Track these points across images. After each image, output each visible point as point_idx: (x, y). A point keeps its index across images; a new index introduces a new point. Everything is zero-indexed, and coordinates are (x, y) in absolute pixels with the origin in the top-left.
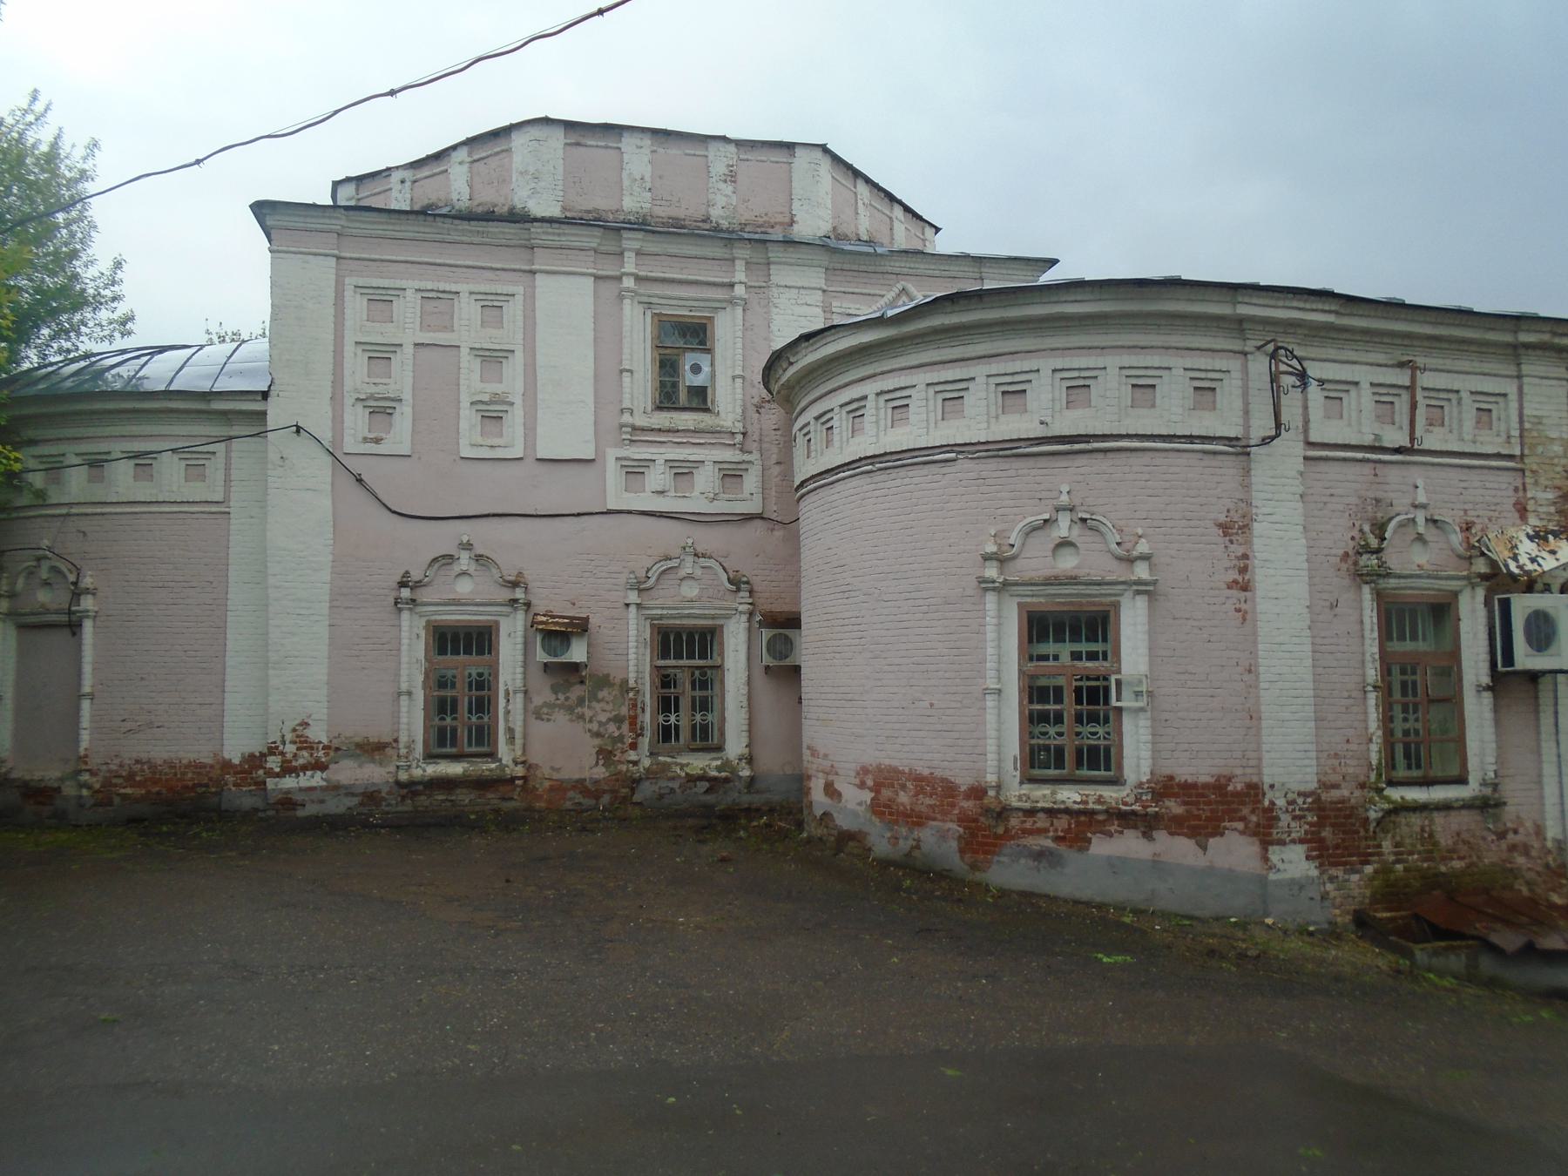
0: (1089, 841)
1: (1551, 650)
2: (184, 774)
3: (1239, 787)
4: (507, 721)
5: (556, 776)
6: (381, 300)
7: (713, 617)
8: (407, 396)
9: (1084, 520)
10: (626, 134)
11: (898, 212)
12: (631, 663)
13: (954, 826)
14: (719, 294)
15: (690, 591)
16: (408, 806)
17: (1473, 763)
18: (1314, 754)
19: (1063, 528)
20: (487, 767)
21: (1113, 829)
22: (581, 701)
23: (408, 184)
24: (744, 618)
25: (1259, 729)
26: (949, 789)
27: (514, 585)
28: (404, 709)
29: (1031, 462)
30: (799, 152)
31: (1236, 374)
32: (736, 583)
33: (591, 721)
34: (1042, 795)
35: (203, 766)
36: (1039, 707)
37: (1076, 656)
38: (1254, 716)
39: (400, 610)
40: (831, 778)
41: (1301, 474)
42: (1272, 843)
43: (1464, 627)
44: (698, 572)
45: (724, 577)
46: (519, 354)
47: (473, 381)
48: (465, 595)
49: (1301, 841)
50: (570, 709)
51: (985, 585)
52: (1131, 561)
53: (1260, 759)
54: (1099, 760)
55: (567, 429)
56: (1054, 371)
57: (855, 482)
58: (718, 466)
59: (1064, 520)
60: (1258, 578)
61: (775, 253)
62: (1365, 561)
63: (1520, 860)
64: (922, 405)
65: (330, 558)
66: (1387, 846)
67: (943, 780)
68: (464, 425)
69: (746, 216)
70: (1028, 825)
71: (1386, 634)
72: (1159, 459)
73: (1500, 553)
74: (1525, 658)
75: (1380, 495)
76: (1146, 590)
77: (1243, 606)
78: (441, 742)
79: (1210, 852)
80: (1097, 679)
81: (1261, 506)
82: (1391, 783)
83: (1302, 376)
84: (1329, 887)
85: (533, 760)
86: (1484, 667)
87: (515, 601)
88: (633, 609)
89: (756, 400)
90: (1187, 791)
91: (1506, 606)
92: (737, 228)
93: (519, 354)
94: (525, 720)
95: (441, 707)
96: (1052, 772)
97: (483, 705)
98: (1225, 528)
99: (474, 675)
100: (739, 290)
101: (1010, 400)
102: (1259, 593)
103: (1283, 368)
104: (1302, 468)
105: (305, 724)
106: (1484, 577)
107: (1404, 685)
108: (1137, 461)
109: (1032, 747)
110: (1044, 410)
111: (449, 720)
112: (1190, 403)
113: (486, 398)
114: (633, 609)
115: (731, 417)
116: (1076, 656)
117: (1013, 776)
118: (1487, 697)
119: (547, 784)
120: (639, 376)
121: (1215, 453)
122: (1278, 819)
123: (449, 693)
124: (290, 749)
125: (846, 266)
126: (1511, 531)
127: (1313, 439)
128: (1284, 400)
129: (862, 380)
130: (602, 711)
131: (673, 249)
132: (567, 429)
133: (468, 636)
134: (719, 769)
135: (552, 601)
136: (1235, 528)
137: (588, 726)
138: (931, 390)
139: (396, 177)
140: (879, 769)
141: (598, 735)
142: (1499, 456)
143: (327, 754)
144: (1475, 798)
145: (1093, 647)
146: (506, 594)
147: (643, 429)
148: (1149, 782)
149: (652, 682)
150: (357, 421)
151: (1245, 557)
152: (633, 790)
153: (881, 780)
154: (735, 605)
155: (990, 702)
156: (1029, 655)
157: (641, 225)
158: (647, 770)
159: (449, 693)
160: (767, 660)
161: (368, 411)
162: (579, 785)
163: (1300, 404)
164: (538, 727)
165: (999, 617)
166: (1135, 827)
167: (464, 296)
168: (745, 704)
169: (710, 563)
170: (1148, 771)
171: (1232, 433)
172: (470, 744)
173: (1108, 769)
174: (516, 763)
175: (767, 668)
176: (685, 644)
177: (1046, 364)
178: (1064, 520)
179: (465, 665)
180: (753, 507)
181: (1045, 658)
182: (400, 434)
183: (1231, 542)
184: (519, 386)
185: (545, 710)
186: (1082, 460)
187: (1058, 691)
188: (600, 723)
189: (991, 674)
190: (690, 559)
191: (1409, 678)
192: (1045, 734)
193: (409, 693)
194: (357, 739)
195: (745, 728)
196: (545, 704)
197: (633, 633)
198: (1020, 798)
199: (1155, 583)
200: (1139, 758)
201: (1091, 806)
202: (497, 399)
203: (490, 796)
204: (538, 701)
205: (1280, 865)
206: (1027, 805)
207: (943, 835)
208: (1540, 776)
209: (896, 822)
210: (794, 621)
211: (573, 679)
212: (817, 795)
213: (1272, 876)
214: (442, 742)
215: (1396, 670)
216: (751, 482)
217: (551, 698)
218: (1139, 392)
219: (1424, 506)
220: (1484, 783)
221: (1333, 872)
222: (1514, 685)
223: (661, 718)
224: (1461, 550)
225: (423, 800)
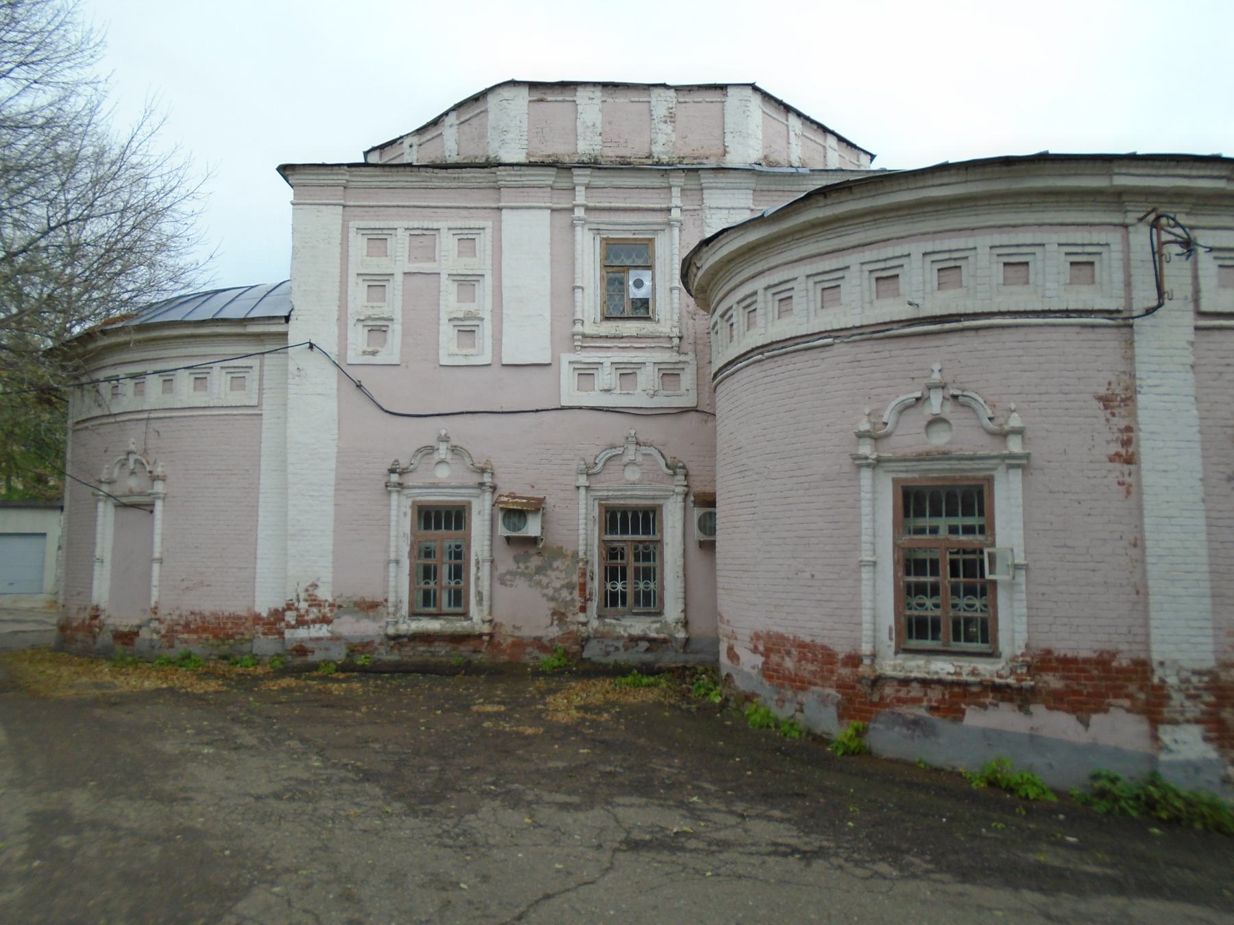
0: (963, 712)
2: (225, 624)
4: (477, 585)
5: (517, 633)
6: (378, 239)
8: (398, 316)
9: (955, 397)
10: (580, 90)
11: (832, 141)
12: (581, 538)
13: (833, 692)
14: (660, 218)
15: (632, 474)
16: (395, 657)
18: (1210, 632)
19: (935, 405)
20: (460, 625)
21: (988, 701)
22: (540, 570)
23: (415, 147)
24: (680, 498)
25: (1146, 605)
26: (829, 657)
27: (483, 471)
28: (392, 575)
29: (903, 343)
30: (730, 91)
31: (1117, 247)
32: (673, 467)
33: (547, 587)
34: (917, 666)
35: (239, 618)
38: (1141, 591)
39: (390, 492)
40: (732, 642)
41: (1192, 343)
42: (1162, 722)
44: (640, 459)
45: (663, 463)
46: (488, 280)
47: (451, 301)
48: (443, 481)
49: (1197, 721)
50: (529, 577)
51: (860, 463)
52: (1004, 435)
53: (1147, 635)
54: (979, 633)
55: (528, 337)
56: (925, 254)
57: (750, 370)
58: (658, 366)
59: (936, 398)
60: (1142, 450)
61: (706, 179)
64: (805, 296)
65: (335, 450)
67: (824, 647)
68: (442, 338)
69: (686, 151)
70: (902, 694)
72: (1033, 335)
76: (1021, 463)
77: (1127, 480)
78: (425, 602)
79: (1092, 729)
80: (974, 552)
83: (1188, 245)
85: (497, 620)
87: (482, 484)
88: (582, 491)
90: (1067, 664)
93: (488, 280)
94: (491, 585)
96: (928, 644)
97: (458, 572)
98: (1106, 401)
100: (676, 214)
101: (884, 285)
103: (1165, 237)
104: (1192, 338)
105: (315, 586)
108: (1006, 335)
109: (910, 619)
110: (921, 291)
111: (432, 584)
112: (1066, 277)
113: (461, 315)
115: (669, 323)
116: (953, 530)
117: (888, 645)
119: (510, 640)
121: (1093, 326)
122: (1169, 697)
124: (303, 605)
125: (773, 187)
127: (1206, 306)
128: (1168, 270)
129: (753, 277)
130: (556, 578)
131: (618, 181)
132: (528, 337)
133: (448, 514)
134: (658, 631)
135: (515, 485)
136: (1119, 400)
137: (545, 591)
138: (811, 281)
139: (407, 142)
140: (769, 635)
141: (552, 599)
143: (331, 611)
146: (476, 479)
147: (592, 337)
148: (1023, 655)
149: (600, 554)
150: (358, 338)
151: (1129, 429)
152: (583, 647)
153: (770, 645)
154: (672, 487)
155: (866, 574)
157: (593, 165)
158: (596, 631)
159: (431, 561)
161: (367, 329)
162: (538, 642)
163: (1189, 273)
164: (501, 591)
165: (874, 492)
166: (1011, 700)
167: (444, 232)
169: (652, 451)
170: (1022, 644)
171: (1112, 306)
172: (450, 605)
174: (484, 622)
176: (630, 522)
177: (916, 248)
178: (936, 398)
179: (443, 538)
180: (689, 401)
181: (921, 531)
182: (392, 350)
183: (1113, 415)
184: (488, 304)
185: (508, 577)
186: (953, 339)
187: (935, 564)
188: (556, 590)
189: (866, 547)
190: (632, 447)
192: (921, 605)
193: (397, 562)
194: (355, 599)
195: (681, 595)
196: (510, 573)
197: (582, 511)
198: (894, 668)
199: (1027, 456)
200: (1013, 631)
201: (965, 677)
202: (469, 316)
203: (462, 648)
204: (502, 569)
205: (1172, 746)
206: (901, 675)
207: (823, 700)
209: (782, 686)
211: (532, 551)
213: (1163, 757)
214: (426, 603)
216: (687, 379)
218: (1011, 270)
223: (609, 586)
225: (407, 651)
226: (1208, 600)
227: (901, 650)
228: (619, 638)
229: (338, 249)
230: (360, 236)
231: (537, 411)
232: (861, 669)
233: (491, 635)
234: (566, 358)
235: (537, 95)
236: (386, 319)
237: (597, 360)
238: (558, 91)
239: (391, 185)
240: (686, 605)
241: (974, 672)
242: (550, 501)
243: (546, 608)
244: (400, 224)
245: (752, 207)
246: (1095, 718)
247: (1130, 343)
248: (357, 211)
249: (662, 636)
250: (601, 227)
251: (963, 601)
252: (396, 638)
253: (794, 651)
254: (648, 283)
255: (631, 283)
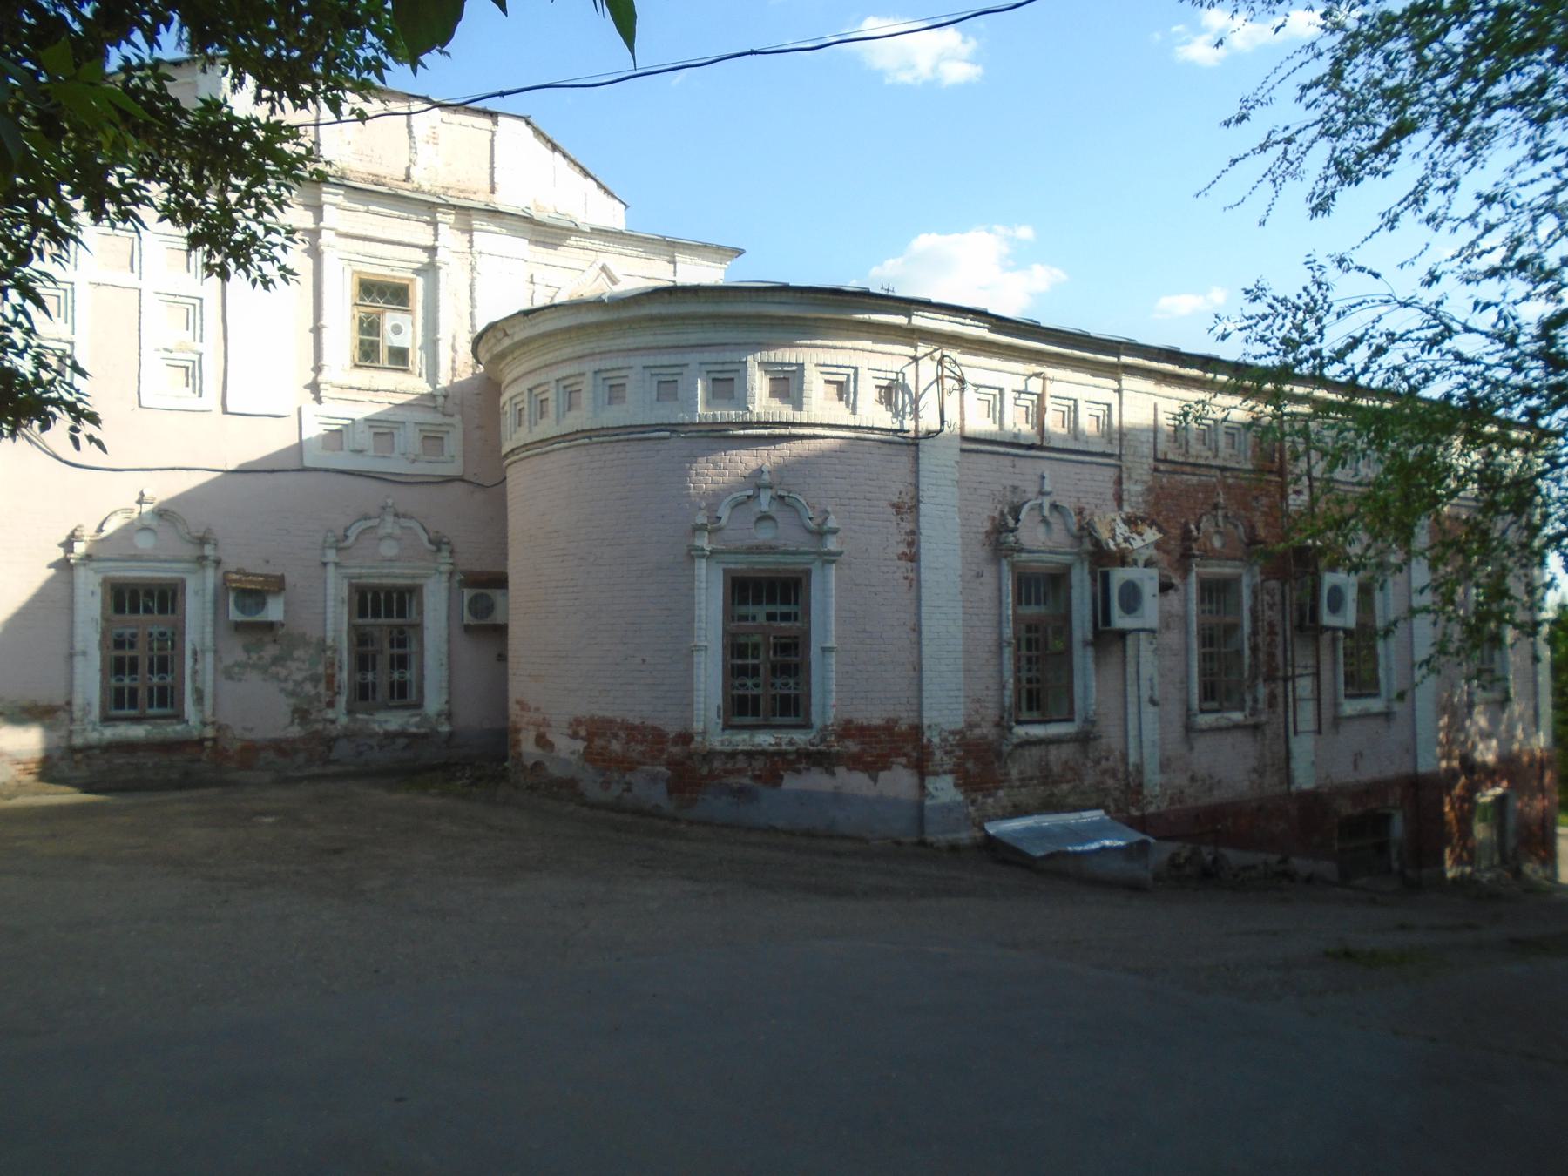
0: (781, 778)
1: (1138, 613)
3: (904, 728)
4: (194, 681)
5: (248, 736)
7: (413, 577)
9: (782, 497)
13: (663, 769)
17: (1078, 704)
18: (961, 700)
20: (173, 730)
22: (276, 661)
24: (445, 578)
26: (659, 736)
32: (438, 543)
33: (286, 680)
36: (740, 662)
37: (771, 617)
38: (918, 668)
43: (1075, 594)
44: (397, 532)
45: (424, 538)
49: (951, 772)
50: (264, 670)
54: (793, 708)
59: (765, 496)
62: (1000, 538)
63: (1110, 782)
66: (1014, 773)
67: (654, 728)
69: (449, 181)
70: (729, 766)
71: (1018, 601)
73: (1104, 534)
74: (1120, 621)
75: (1017, 483)
77: (911, 575)
78: (119, 702)
79: (880, 783)
81: (926, 491)
82: (1019, 723)
83: (962, 381)
84: (971, 809)
86: (1088, 625)
87: (204, 558)
91: (1106, 578)
92: (440, 191)
94: (215, 681)
95: (119, 665)
96: (749, 720)
98: (897, 507)
99: (156, 634)
102: (923, 564)
103: (946, 372)
106: (1092, 554)
107: (1029, 641)
111: (127, 681)
114: (331, 569)
117: (715, 722)
118: (1090, 652)
119: (238, 745)
122: (932, 754)
123: (127, 653)
126: (1112, 515)
130: (297, 669)
133: (149, 594)
134: (417, 725)
137: (283, 685)
138: (647, 372)
140: (592, 720)
141: (293, 694)
142: (1104, 455)
144: (1077, 734)
145: (785, 609)
146: (190, 551)
149: (350, 640)
151: (913, 533)
152: (330, 749)
153: (594, 730)
156: (729, 616)
159: (127, 653)
160: (468, 619)
168: (445, 661)
169: (412, 524)
173: (797, 714)
175: (468, 629)
176: (383, 607)
178: (765, 496)
179: (146, 624)
181: (744, 618)
188: (297, 683)
190: (390, 519)
191: (1033, 635)
193: (84, 653)
195: (444, 685)
196: (237, 664)
199: (841, 553)
204: (228, 661)
206: (728, 749)
207: (654, 779)
208: (1126, 714)
210: (500, 581)
212: (528, 746)
214: (119, 704)
215: (1023, 627)
217: (241, 656)
219: (1048, 494)
220: (1086, 720)
221: (973, 796)
222: (1107, 639)
224: (1075, 528)
226: (961, 674)
227: (727, 726)
228: (374, 735)
231: (273, 471)
232: (692, 746)
233: (214, 740)
240: (450, 694)
241: (791, 743)
242: (289, 580)
243: (284, 705)
246: (883, 775)
247: (916, 459)
249: (423, 731)
251: (779, 682)
252: (87, 748)
253: (622, 734)
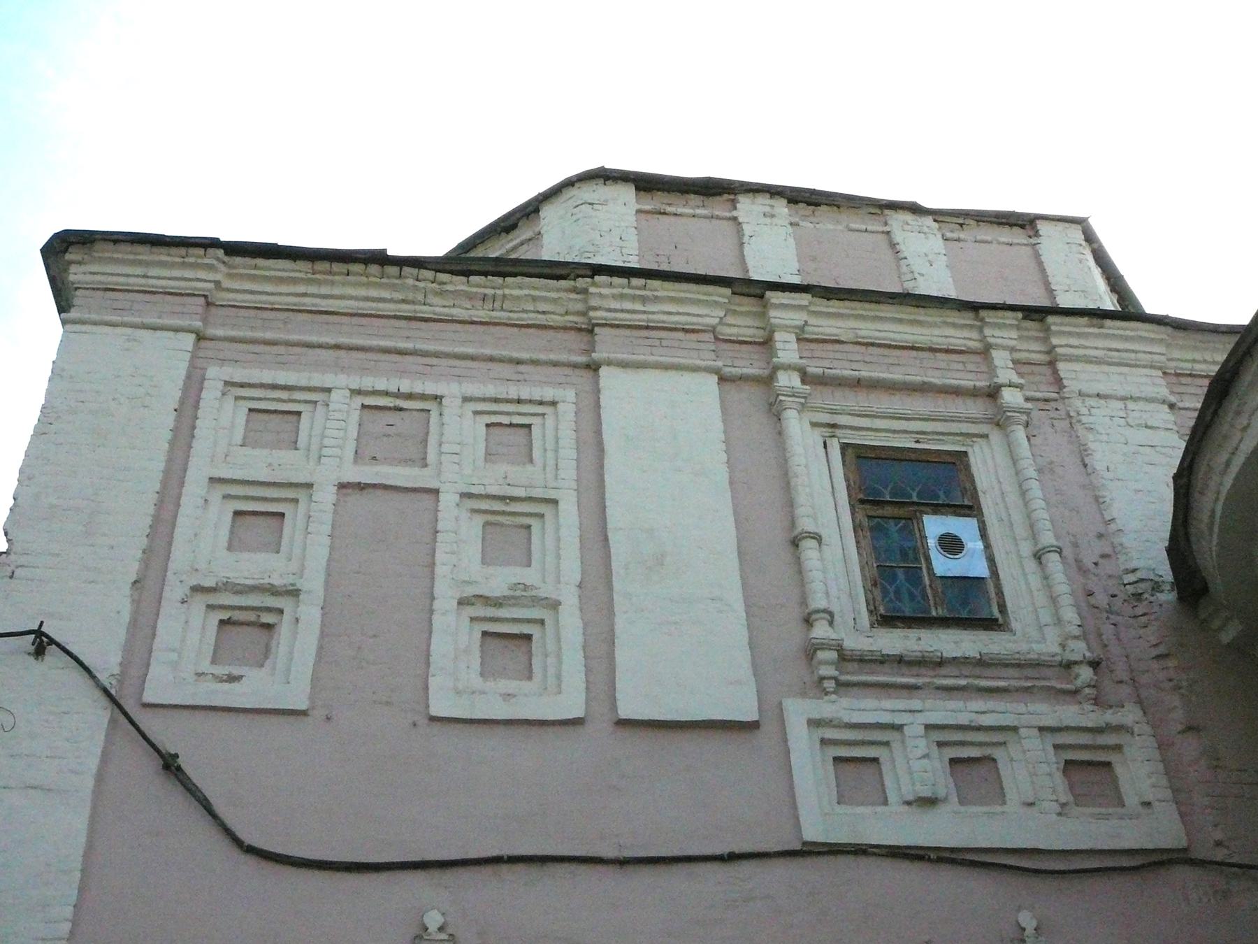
6: (276, 416)
14: (975, 408)
55: (689, 643)
58: (1051, 739)
68: (440, 646)
89: (1101, 599)
120: (833, 550)
132: (689, 643)
150: (185, 636)
180: (1162, 829)
182: (286, 676)
184: (572, 568)
216: (1138, 772)
229: (170, 420)
230: (229, 403)
234: (798, 711)
235: (649, 203)
236: (273, 591)
237: (886, 718)
238: (694, 199)
239: (325, 305)
244: (341, 381)
245: (1173, 399)
248: (230, 350)
250: (843, 420)
254: (974, 544)
255: (932, 542)
